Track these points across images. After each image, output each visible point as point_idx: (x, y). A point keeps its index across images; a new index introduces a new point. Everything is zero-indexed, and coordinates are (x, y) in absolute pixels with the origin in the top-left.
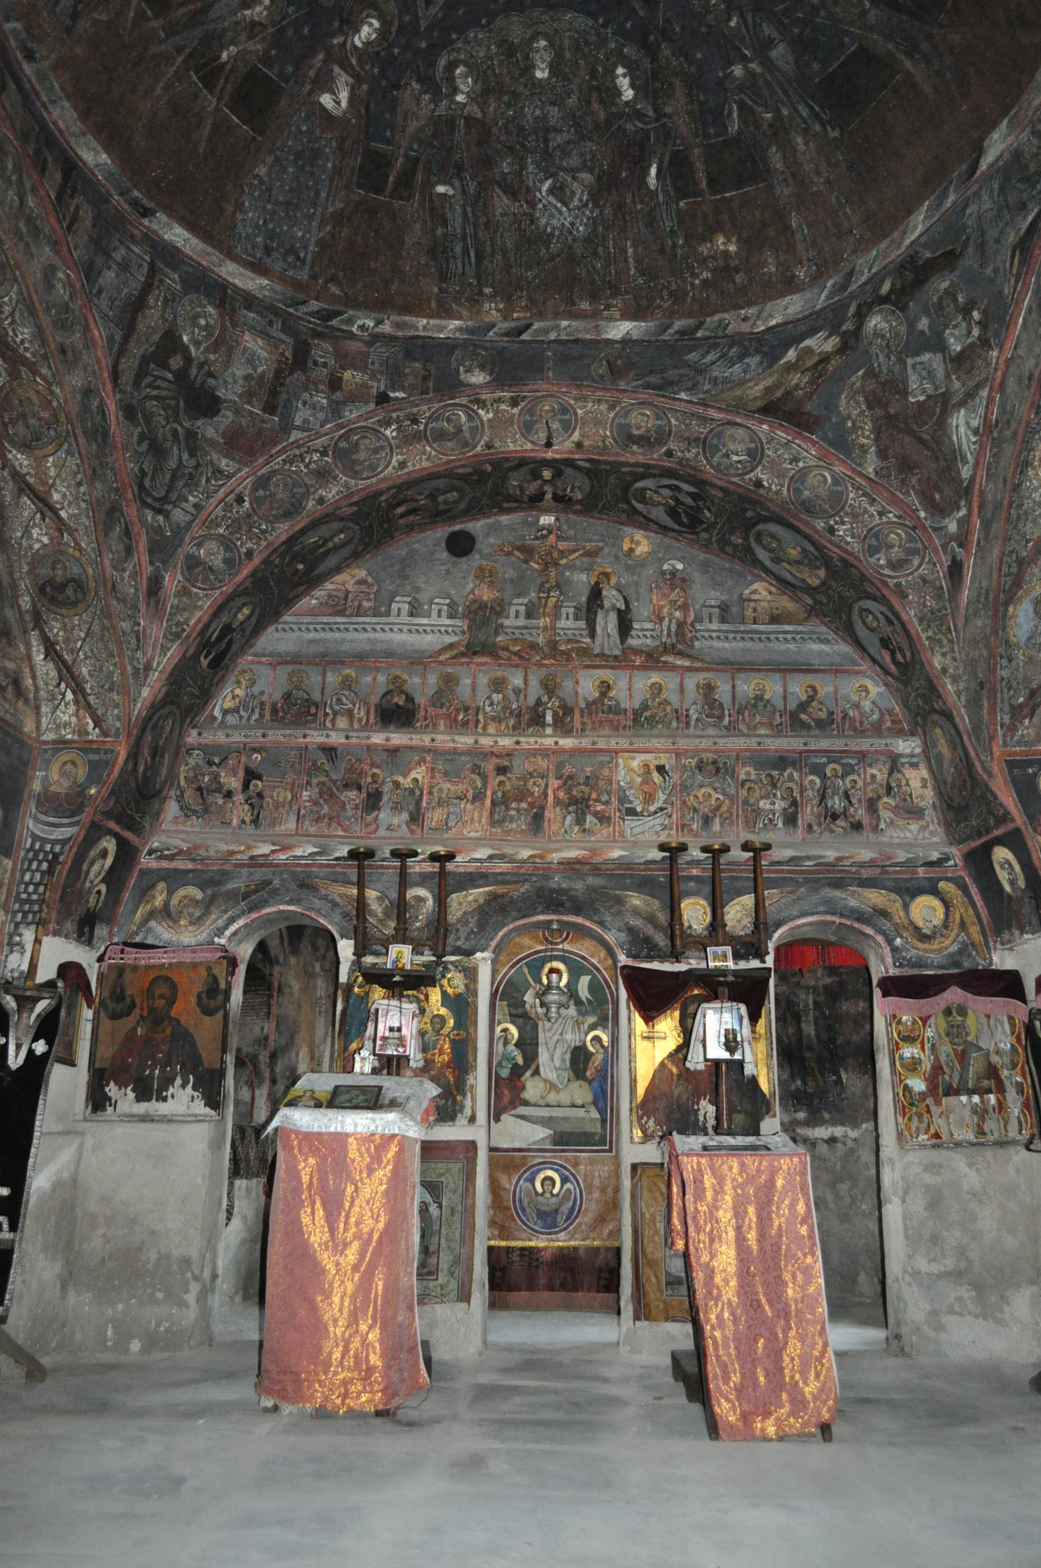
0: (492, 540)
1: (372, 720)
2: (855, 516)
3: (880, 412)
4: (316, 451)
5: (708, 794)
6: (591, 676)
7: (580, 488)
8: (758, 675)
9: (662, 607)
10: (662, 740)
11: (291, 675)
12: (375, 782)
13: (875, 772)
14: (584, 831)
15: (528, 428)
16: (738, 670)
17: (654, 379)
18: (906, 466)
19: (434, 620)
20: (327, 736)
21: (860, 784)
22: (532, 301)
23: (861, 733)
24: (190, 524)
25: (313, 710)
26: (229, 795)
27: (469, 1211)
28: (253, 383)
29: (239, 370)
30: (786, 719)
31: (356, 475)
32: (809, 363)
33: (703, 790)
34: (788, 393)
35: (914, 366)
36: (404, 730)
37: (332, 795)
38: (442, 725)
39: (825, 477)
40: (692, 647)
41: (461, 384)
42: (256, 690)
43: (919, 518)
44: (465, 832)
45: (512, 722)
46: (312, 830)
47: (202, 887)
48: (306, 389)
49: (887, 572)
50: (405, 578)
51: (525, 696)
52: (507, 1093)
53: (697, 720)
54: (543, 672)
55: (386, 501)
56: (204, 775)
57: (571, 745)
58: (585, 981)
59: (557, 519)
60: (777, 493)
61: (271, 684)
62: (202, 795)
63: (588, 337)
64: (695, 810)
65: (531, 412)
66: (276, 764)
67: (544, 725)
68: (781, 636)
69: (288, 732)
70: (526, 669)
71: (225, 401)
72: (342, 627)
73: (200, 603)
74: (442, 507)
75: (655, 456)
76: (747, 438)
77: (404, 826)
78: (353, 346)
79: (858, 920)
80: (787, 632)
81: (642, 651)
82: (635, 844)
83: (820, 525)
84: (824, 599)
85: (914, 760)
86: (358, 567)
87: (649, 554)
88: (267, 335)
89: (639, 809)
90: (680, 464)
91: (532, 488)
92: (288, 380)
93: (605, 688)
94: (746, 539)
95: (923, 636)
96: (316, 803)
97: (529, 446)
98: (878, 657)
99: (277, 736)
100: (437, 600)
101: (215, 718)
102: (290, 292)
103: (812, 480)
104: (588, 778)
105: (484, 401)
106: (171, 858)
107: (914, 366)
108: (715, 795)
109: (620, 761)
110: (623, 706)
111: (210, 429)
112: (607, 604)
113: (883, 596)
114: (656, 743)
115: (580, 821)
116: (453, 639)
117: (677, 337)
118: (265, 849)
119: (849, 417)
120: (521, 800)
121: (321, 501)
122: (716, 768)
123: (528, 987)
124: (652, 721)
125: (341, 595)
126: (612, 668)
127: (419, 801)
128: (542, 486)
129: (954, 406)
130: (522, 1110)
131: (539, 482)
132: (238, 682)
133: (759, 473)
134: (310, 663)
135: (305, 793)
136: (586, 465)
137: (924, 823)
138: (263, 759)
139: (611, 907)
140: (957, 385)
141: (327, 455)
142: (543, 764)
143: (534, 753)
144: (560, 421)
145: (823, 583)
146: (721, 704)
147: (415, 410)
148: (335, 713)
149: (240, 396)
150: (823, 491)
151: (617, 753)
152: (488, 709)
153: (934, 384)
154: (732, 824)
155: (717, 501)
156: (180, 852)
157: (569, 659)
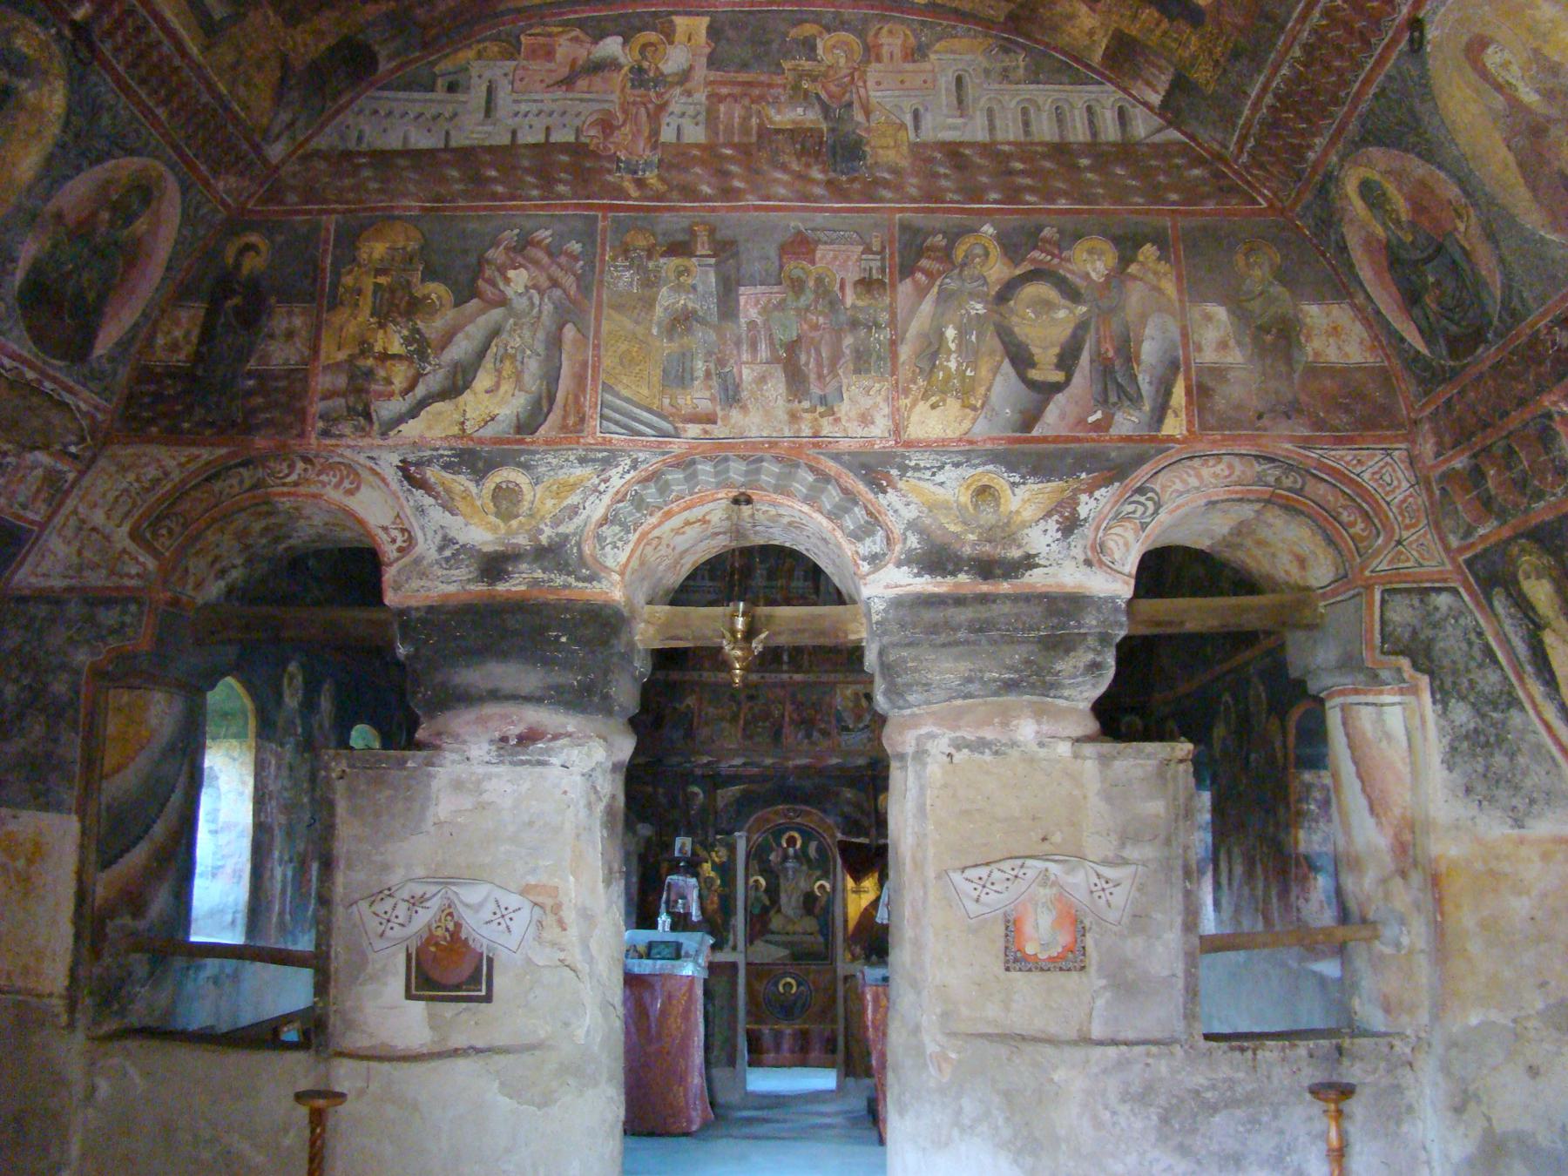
27: (733, 1007)
38: (707, 665)
52: (758, 926)
58: (813, 846)
67: (781, 662)
115: (808, 736)
123: (772, 849)
130: (769, 937)
143: (775, 685)
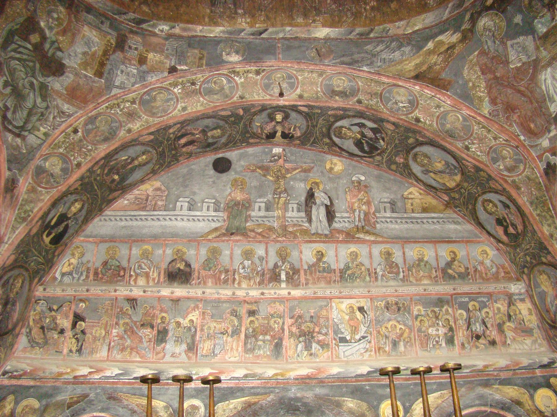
0: (242, 163)
1: (162, 279)
2: (481, 140)
3: (489, 76)
4: (128, 101)
5: (394, 325)
6: (310, 248)
7: (299, 128)
8: (418, 245)
9: (354, 203)
10: (361, 290)
11: (108, 250)
12: (163, 322)
13: (499, 305)
14: (311, 355)
15: (267, 87)
16: (405, 242)
17: (346, 59)
18: (510, 108)
19: (204, 213)
20: (131, 291)
21: (491, 314)
22: (268, 18)
23: (487, 280)
24: (40, 145)
25: (122, 273)
26: (62, 332)
28: (88, 57)
29: (79, 48)
30: (439, 274)
31: (153, 115)
32: (442, 49)
33: (391, 323)
34: (430, 68)
35: (512, 46)
36: (184, 286)
37: (133, 332)
38: (210, 283)
39: (458, 117)
40: (375, 228)
41: (223, 62)
42: (85, 260)
43: (520, 140)
44: (227, 357)
45: (258, 280)
46: (119, 357)
47: (39, 398)
48: (123, 63)
49: (505, 173)
50: (186, 186)
51: (267, 262)
53: (382, 276)
54: (278, 245)
55: (174, 133)
56: (46, 317)
57: (299, 295)
59: (284, 150)
60: (430, 125)
61: (95, 255)
62: (44, 331)
63: (303, 36)
64: (387, 337)
65: (268, 78)
66: (95, 310)
68: (430, 220)
69: (104, 288)
70: (267, 243)
71: (69, 67)
72: (143, 218)
73: (42, 198)
74: (210, 141)
75: (350, 103)
76: (407, 94)
77: (184, 355)
78: (154, 40)
79: (502, 409)
80: (433, 218)
81: (343, 231)
82: (347, 362)
83: (460, 145)
84: (457, 196)
85: (522, 297)
86: (156, 180)
87: (343, 170)
88: (99, 28)
89: (348, 338)
90: (367, 107)
91: (269, 128)
92: (112, 57)
93: (320, 255)
94: (406, 159)
95: (534, 214)
96: (122, 338)
97: (268, 97)
98: (493, 232)
99: (97, 290)
100: (206, 200)
101: (55, 279)
102: (116, 7)
103: (451, 118)
104: (312, 317)
105: (238, 72)
106: (19, 377)
107: (512, 46)
108: (399, 326)
109: (333, 304)
110: (333, 267)
111: (57, 84)
112: (318, 201)
113: (504, 189)
114: (356, 292)
115: (308, 347)
116: (217, 225)
117: (358, 37)
118: (84, 371)
119: (470, 80)
120: (266, 334)
121: (129, 131)
122: (398, 307)
124: (352, 277)
125: (144, 197)
126: (324, 242)
127: (193, 336)
128: (275, 126)
129: (543, 67)
131: (273, 123)
132: (73, 255)
133: (416, 113)
134: (121, 241)
135: (114, 331)
136: (305, 109)
137: (534, 338)
138: (86, 307)
139: (333, 410)
140: (544, 53)
141: (135, 104)
142: (280, 308)
143: (274, 300)
144: (288, 83)
145: (458, 185)
146: (397, 264)
147: (194, 77)
148: (137, 275)
149: (79, 65)
150: (458, 125)
151: (331, 299)
152: (241, 271)
153: (527, 55)
154: (411, 346)
155: (390, 133)
156: (25, 373)
157: (295, 237)
